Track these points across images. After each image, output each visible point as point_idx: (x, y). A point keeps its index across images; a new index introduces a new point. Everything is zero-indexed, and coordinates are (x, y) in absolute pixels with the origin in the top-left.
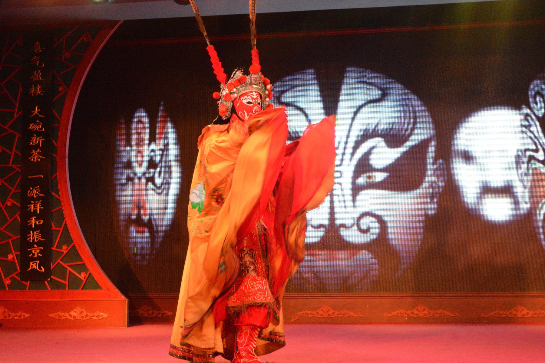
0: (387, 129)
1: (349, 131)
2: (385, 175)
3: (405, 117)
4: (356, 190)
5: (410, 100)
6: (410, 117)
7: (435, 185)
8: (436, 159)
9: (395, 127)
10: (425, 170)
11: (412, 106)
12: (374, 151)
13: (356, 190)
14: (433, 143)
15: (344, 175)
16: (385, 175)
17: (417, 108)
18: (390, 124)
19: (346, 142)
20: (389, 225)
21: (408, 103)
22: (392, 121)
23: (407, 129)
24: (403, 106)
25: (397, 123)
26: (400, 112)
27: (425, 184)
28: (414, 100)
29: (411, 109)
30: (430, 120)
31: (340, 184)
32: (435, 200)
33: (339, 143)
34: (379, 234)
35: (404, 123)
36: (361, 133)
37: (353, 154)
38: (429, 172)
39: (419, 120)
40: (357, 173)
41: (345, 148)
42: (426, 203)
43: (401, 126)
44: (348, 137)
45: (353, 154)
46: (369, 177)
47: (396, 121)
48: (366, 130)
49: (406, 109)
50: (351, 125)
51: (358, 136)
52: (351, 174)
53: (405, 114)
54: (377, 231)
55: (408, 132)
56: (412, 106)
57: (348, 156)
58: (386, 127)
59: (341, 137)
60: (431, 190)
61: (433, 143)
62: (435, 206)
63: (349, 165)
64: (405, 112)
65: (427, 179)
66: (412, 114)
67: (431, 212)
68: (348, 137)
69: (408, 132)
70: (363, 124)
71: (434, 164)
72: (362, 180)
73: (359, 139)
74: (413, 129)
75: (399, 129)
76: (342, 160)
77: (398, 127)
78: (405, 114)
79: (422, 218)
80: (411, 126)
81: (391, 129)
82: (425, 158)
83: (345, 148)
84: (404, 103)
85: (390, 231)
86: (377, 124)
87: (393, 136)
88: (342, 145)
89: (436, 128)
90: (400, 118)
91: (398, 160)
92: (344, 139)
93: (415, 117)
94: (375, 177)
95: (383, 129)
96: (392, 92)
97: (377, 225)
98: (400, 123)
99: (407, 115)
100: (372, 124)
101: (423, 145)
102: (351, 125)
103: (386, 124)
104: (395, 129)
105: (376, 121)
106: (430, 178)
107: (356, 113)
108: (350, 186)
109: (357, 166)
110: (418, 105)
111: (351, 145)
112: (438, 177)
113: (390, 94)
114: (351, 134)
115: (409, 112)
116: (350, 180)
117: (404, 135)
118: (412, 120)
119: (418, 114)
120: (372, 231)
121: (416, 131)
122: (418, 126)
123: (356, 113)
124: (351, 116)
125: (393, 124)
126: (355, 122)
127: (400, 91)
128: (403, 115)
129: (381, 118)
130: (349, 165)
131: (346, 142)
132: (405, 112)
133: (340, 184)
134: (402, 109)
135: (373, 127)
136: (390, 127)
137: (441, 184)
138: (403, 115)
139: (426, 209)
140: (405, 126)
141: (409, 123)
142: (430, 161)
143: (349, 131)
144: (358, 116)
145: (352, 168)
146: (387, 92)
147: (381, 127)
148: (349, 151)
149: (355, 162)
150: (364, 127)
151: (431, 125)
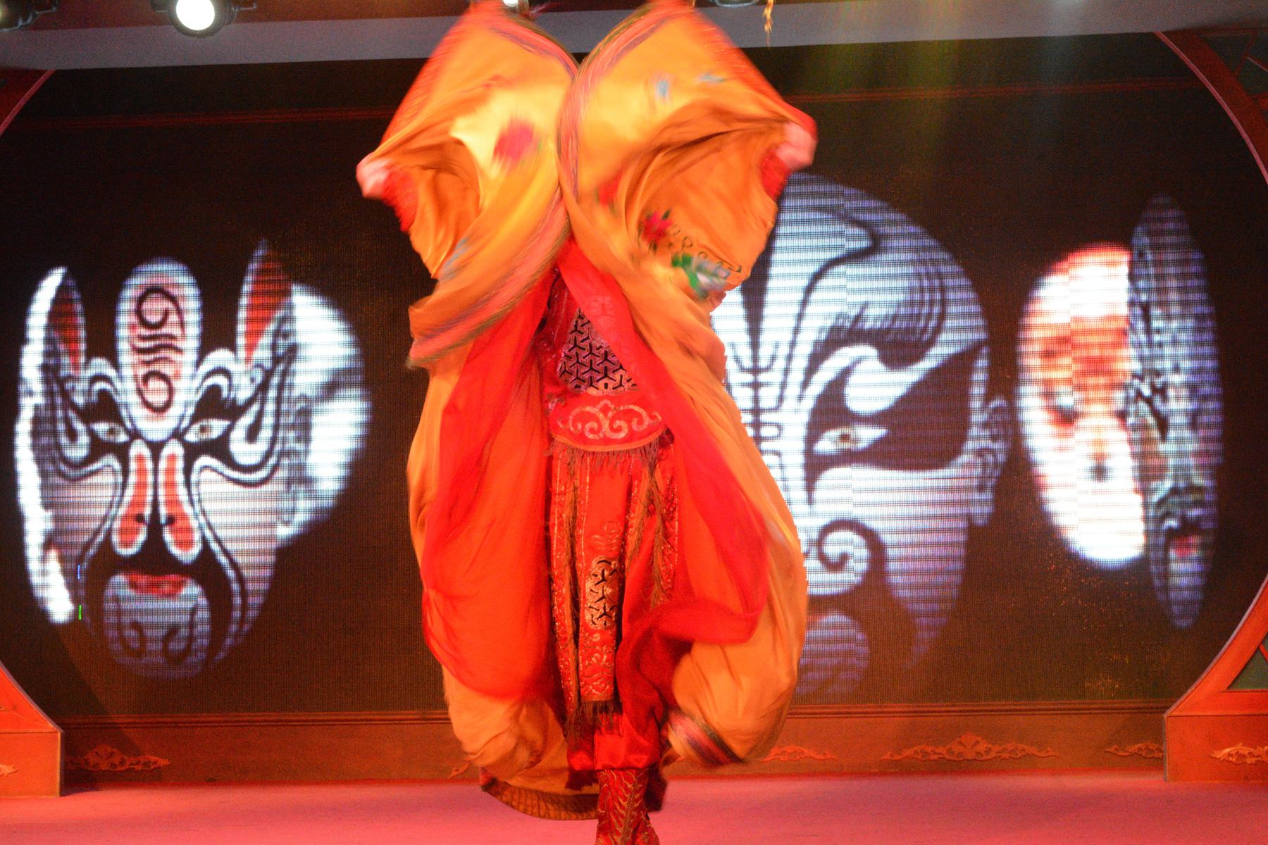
1: (796, 330)
3: (922, 303)
4: (815, 466)
5: (934, 262)
6: (932, 303)
7: (990, 458)
8: (988, 398)
9: (897, 324)
10: (965, 425)
11: (940, 276)
12: (853, 380)
13: (815, 466)
14: (982, 363)
15: (786, 432)
17: (949, 282)
18: (886, 317)
19: (790, 358)
20: (891, 552)
21: (932, 270)
22: (892, 311)
23: (924, 329)
24: (918, 276)
25: (903, 316)
26: (912, 289)
27: (964, 459)
28: (945, 262)
29: (936, 283)
30: (975, 308)
31: (778, 453)
32: (988, 495)
33: (773, 358)
34: (868, 575)
36: (823, 336)
37: (805, 384)
38: (974, 431)
39: (952, 309)
40: (815, 430)
41: (787, 371)
42: (968, 503)
43: (913, 324)
44: (793, 344)
45: (805, 384)
46: (845, 438)
47: (902, 311)
49: (926, 283)
50: (800, 317)
51: (816, 343)
52: (802, 432)
53: (922, 296)
54: (862, 567)
55: (927, 337)
56: (940, 276)
57: (793, 390)
58: (878, 325)
59: (777, 345)
61: (982, 363)
62: (987, 509)
63: (797, 411)
64: (922, 290)
65: (970, 445)
66: (938, 296)
67: (980, 522)
68: (793, 344)
69: (927, 337)
70: (828, 316)
71: (983, 409)
72: (827, 444)
74: (938, 330)
76: (781, 399)
77: (904, 325)
78: (922, 296)
79: (961, 538)
80: (933, 323)
81: (888, 330)
82: (966, 397)
83: (787, 371)
84: (922, 270)
85: (893, 566)
86: (858, 318)
87: (898, 344)
88: (780, 364)
89: (988, 328)
90: (911, 303)
91: (902, 400)
92: (784, 351)
93: (944, 303)
94: (856, 440)
96: (894, 243)
98: (910, 317)
101: (958, 366)
102: (800, 317)
103: (877, 318)
104: (899, 329)
105: (854, 312)
106: (977, 439)
107: (809, 290)
108: (800, 459)
109: (815, 413)
110: (953, 275)
111: (800, 363)
112: (994, 438)
113: (886, 250)
114: (801, 337)
115: (932, 289)
116: (801, 445)
117: (919, 340)
118: (937, 310)
119: (951, 296)
121: (944, 337)
122: (949, 323)
123: (809, 290)
124: (800, 296)
125: (895, 317)
126: (809, 310)
127: (916, 243)
128: (917, 297)
129: (865, 305)
131: (790, 358)
132: (922, 290)
133: (778, 453)
134: (916, 283)
135: (848, 324)
136: (887, 324)
137: (1001, 458)
138: (917, 297)
139: (969, 518)
140: (922, 324)
141: (929, 316)
142: (976, 404)
143: (796, 330)
144: (815, 296)
145: (805, 418)
146: (884, 243)
147: (868, 325)
148: (797, 376)
149: (809, 403)
150: (829, 323)
151: (979, 322)
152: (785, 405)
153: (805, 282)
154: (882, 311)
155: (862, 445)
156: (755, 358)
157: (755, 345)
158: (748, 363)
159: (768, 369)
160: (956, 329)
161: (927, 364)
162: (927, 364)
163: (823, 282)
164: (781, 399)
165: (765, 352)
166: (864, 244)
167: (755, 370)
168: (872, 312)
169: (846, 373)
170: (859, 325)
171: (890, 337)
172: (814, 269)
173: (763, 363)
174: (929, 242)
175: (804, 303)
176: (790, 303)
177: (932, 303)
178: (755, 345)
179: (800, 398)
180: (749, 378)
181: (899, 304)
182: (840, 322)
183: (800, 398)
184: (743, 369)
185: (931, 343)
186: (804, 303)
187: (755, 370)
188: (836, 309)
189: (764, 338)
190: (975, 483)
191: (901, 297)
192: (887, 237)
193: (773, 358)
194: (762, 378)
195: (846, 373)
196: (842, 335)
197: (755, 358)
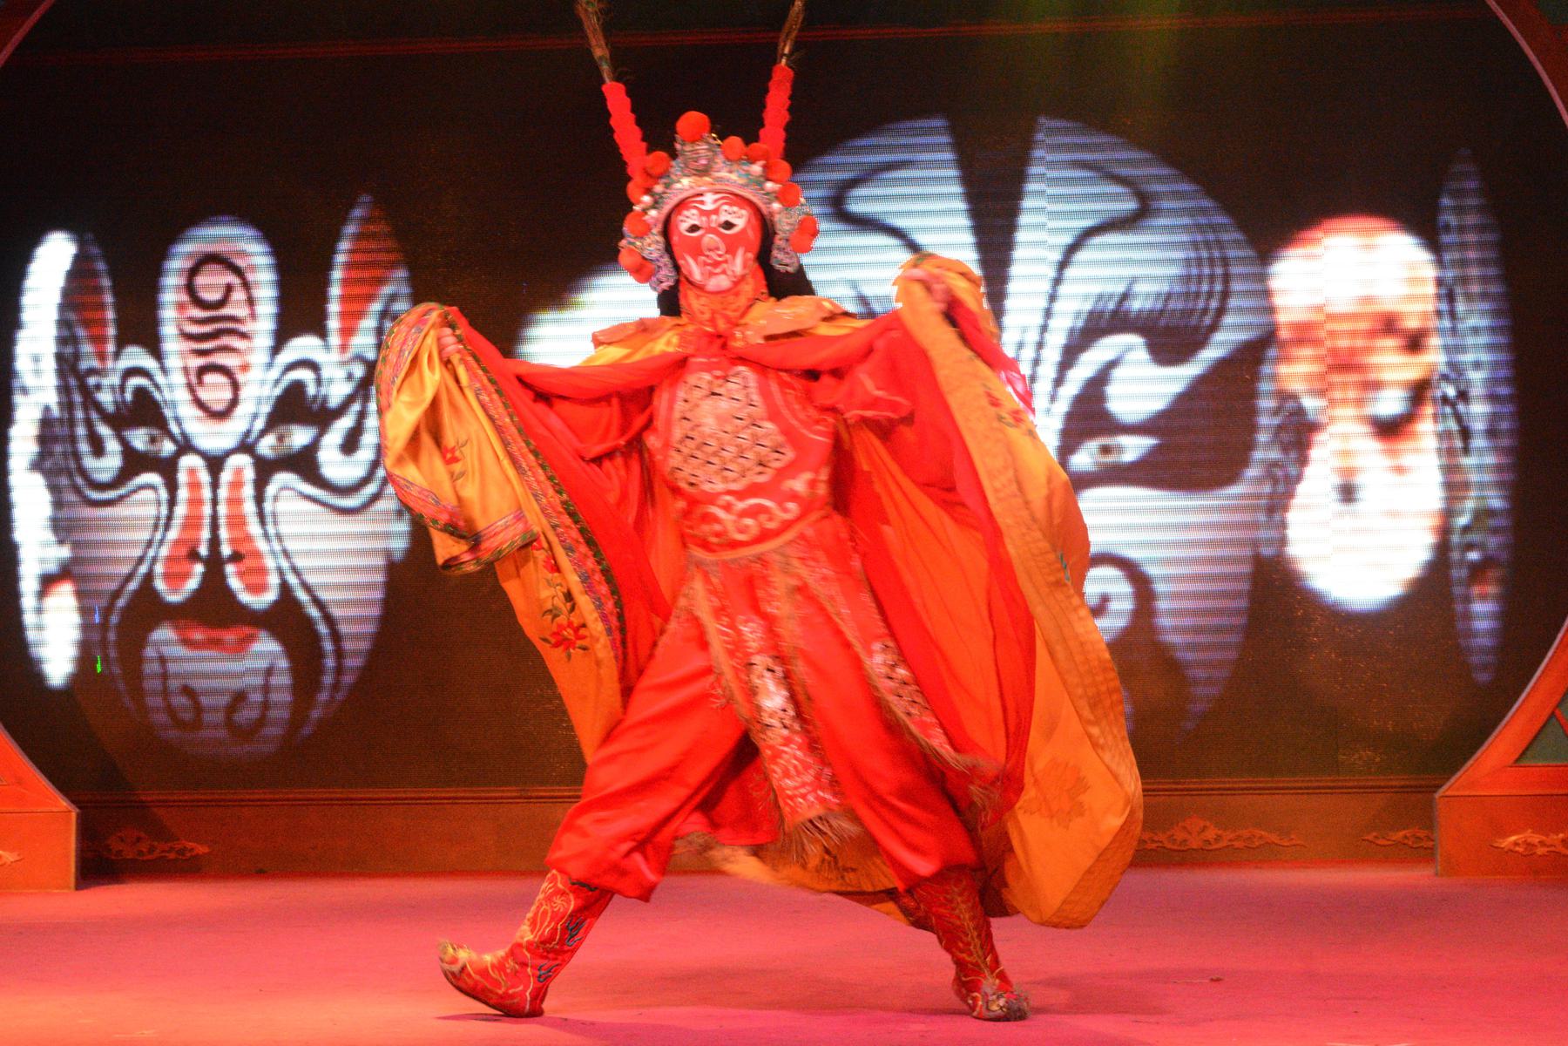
0: (1151, 311)
1: (1048, 313)
2: (1146, 442)
3: (1200, 278)
5: (1214, 228)
6: (1212, 278)
9: (1172, 305)
10: (1253, 428)
11: (1220, 244)
12: (1117, 373)
16: (1146, 442)
17: (1232, 253)
18: (1158, 295)
19: (1040, 345)
20: (1160, 587)
21: (1211, 237)
22: (1165, 288)
23: (1205, 311)
24: (1195, 245)
25: (1179, 294)
26: (1187, 262)
27: (1252, 472)
29: (1216, 254)
35: (1197, 295)
36: (1080, 324)
37: (1059, 381)
38: (1263, 437)
39: (1236, 286)
40: (1071, 438)
42: (1255, 525)
45: (1059, 381)
46: (1105, 450)
47: (1177, 288)
48: (1091, 313)
49: (1205, 254)
51: (1072, 331)
55: (1207, 320)
58: (1148, 305)
59: (1024, 330)
65: (1258, 455)
70: (1086, 297)
74: (1221, 311)
75: (1183, 311)
80: (1214, 304)
81: (1162, 312)
84: (1199, 238)
85: (1162, 605)
86: (1125, 296)
87: (1169, 331)
90: (1186, 279)
92: (1033, 337)
93: (1227, 278)
94: (1120, 449)
95: (1140, 311)
96: (1166, 204)
98: (1187, 294)
99: (1206, 271)
100: (1111, 296)
102: (1053, 298)
103: (1148, 295)
105: (1120, 289)
107: (1063, 265)
109: (1070, 417)
111: (1052, 355)
113: (1158, 212)
115: (1211, 261)
118: (1218, 287)
119: (1235, 270)
120: (1114, 606)
121: (1228, 319)
122: (1233, 302)
123: (1063, 265)
124: (1052, 273)
125: (1169, 296)
126: (1063, 289)
128: (1194, 271)
131: (1040, 345)
132: (1199, 261)
134: (1192, 254)
135: (1111, 306)
136: (1159, 305)
139: (1255, 543)
140: (1201, 304)
141: (1210, 294)
143: (1048, 313)
144: (1069, 272)
146: (1155, 205)
147: (1136, 305)
149: (1063, 406)
150: (1088, 306)
153: (1057, 256)
154: (1154, 288)
155: (1129, 457)
161: (1210, 354)
162: (1210, 354)
163: (1081, 256)
166: (1130, 205)
168: (1140, 288)
169: (1113, 364)
170: (1127, 304)
171: (1162, 322)
174: (1207, 203)
175: (1057, 281)
176: (1041, 277)
177: (1212, 278)
179: (1053, 398)
181: (1171, 279)
182: (1100, 306)
185: (1214, 327)
186: (1057, 281)
188: (1097, 289)
190: (1263, 502)
191: (1175, 271)
192: (1156, 196)
193: (1020, 345)
195: (1113, 364)
196: (1103, 324)
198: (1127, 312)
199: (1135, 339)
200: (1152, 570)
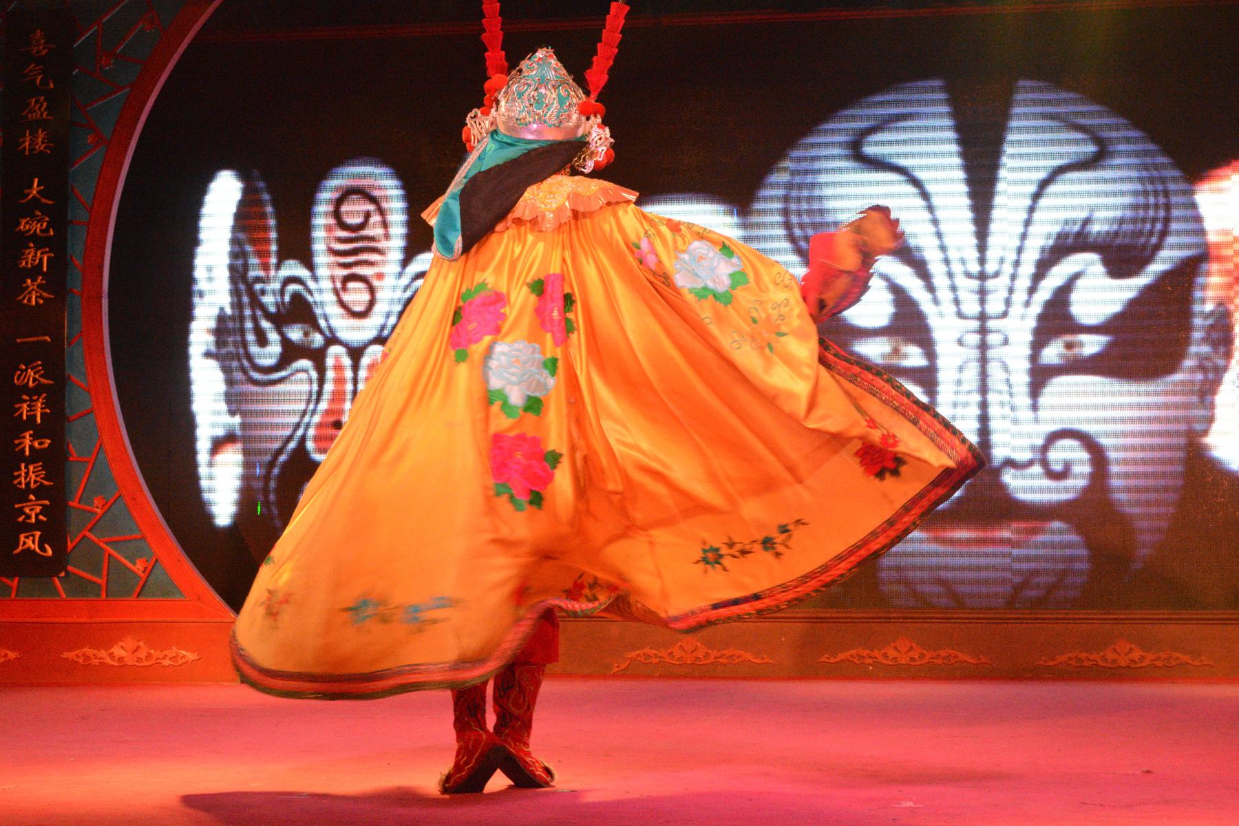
0: (1107, 233)
1: (1024, 236)
3: (1146, 207)
5: (1157, 167)
9: (1125, 227)
10: (1188, 328)
11: (1162, 180)
12: (1080, 283)
17: (1172, 187)
18: (1113, 221)
19: (1017, 263)
20: (1112, 455)
21: (1155, 174)
22: (1118, 214)
23: (1151, 233)
26: (1136, 193)
27: (1189, 363)
36: (1051, 242)
37: (1032, 290)
38: (1197, 335)
41: (1014, 277)
43: (1139, 226)
44: (1020, 250)
45: (1032, 290)
47: (1128, 214)
50: (1028, 223)
51: (1043, 250)
54: (1087, 469)
55: (1154, 240)
57: (1020, 296)
58: (1106, 228)
60: (1199, 376)
63: (1023, 317)
65: (1193, 349)
68: (1020, 250)
69: (1154, 240)
70: (1055, 222)
73: (1046, 255)
74: (1164, 233)
76: (1008, 302)
80: (1159, 226)
81: (1116, 234)
83: (1014, 277)
86: (1087, 221)
87: (1123, 248)
88: (1008, 269)
90: (1136, 207)
93: (1168, 207)
94: (1080, 344)
95: (1099, 233)
96: (1121, 147)
97: (1084, 455)
100: (1074, 222)
102: (1028, 223)
103: (1104, 221)
105: (1083, 215)
107: (1037, 196)
109: (1041, 318)
111: (1028, 269)
113: (1113, 155)
114: (1028, 243)
115: (1156, 193)
116: (1027, 351)
117: (1144, 246)
120: (1076, 469)
121: (1170, 240)
122: (1174, 226)
123: (1037, 196)
124: (1028, 202)
125: (1121, 221)
126: (1037, 216)
129: (1093, 208)
130: (1023, 317)
131: (1017, 263)
135: (1076, 228)
136: (1115, 227)
140: (1148, 226)
143: (1024, 236)
144: (1042, 202)
146: (1111, 148)
147: (1095, 228)
148: (1024, 282)
149: (1036, 309)
150: (1057, 229)
152: (1012, 311)
153: (1033, 189)
156: (982, 261)
157: (982, 248)
158: (975, 268)
159: (997, 274)
160: (1179, 233)
161: (1156, 268)
162: (1156, 268)
163: (1052, 189)
164: (1008, 302)
165: (992, 254)
166: (1091, 148)
167: (982, 277)
168: (1099, 215)
169: (1076, 276)
172: (1042, 175)
173: (990, 268)
175: (1032, 210)
178: (982, 248)
179: (1027, 304)
180: (975, 284)
182: (1067, 228)
183: (1027, 304)
184: (969, 275)
185: (1158, 247)
186: (1032, 210)
187: (982, 277)
189: (991, 240)
190: (1196, 387)
193: (1002, 261)
194: (990, 284)
195: (1076, 276)
196: (1070, 241)
197: (982, 261)
198: (1088, 234)
199: (1093, 257)
200: (1105, 441)
